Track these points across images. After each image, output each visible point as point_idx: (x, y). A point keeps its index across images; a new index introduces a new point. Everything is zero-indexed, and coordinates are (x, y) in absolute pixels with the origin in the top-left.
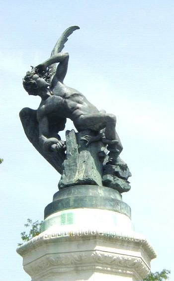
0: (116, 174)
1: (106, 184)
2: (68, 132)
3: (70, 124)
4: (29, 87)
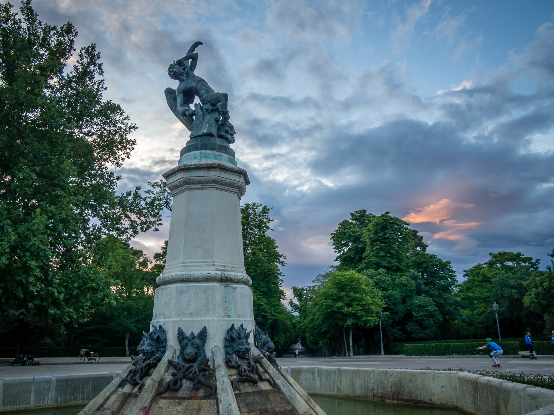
0: (227, 131)
1: (220, 137)
2: (196, 105)
3: (197, 100)
4: (172, 74)
